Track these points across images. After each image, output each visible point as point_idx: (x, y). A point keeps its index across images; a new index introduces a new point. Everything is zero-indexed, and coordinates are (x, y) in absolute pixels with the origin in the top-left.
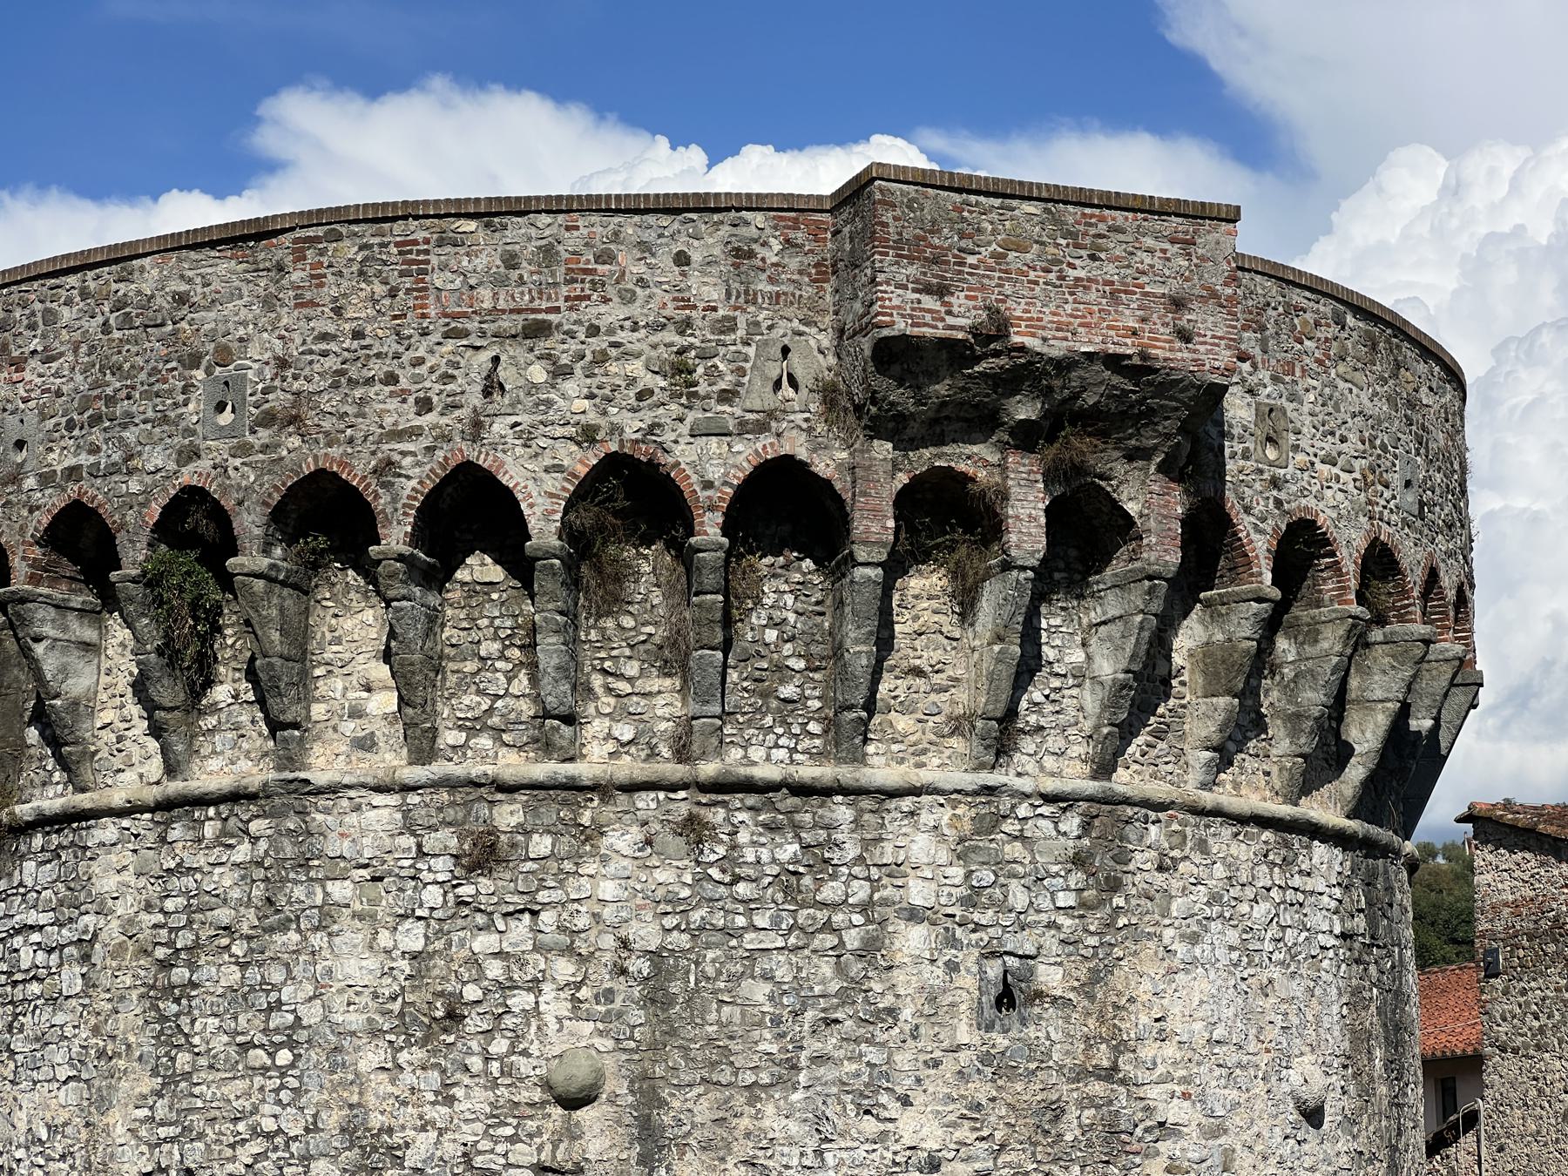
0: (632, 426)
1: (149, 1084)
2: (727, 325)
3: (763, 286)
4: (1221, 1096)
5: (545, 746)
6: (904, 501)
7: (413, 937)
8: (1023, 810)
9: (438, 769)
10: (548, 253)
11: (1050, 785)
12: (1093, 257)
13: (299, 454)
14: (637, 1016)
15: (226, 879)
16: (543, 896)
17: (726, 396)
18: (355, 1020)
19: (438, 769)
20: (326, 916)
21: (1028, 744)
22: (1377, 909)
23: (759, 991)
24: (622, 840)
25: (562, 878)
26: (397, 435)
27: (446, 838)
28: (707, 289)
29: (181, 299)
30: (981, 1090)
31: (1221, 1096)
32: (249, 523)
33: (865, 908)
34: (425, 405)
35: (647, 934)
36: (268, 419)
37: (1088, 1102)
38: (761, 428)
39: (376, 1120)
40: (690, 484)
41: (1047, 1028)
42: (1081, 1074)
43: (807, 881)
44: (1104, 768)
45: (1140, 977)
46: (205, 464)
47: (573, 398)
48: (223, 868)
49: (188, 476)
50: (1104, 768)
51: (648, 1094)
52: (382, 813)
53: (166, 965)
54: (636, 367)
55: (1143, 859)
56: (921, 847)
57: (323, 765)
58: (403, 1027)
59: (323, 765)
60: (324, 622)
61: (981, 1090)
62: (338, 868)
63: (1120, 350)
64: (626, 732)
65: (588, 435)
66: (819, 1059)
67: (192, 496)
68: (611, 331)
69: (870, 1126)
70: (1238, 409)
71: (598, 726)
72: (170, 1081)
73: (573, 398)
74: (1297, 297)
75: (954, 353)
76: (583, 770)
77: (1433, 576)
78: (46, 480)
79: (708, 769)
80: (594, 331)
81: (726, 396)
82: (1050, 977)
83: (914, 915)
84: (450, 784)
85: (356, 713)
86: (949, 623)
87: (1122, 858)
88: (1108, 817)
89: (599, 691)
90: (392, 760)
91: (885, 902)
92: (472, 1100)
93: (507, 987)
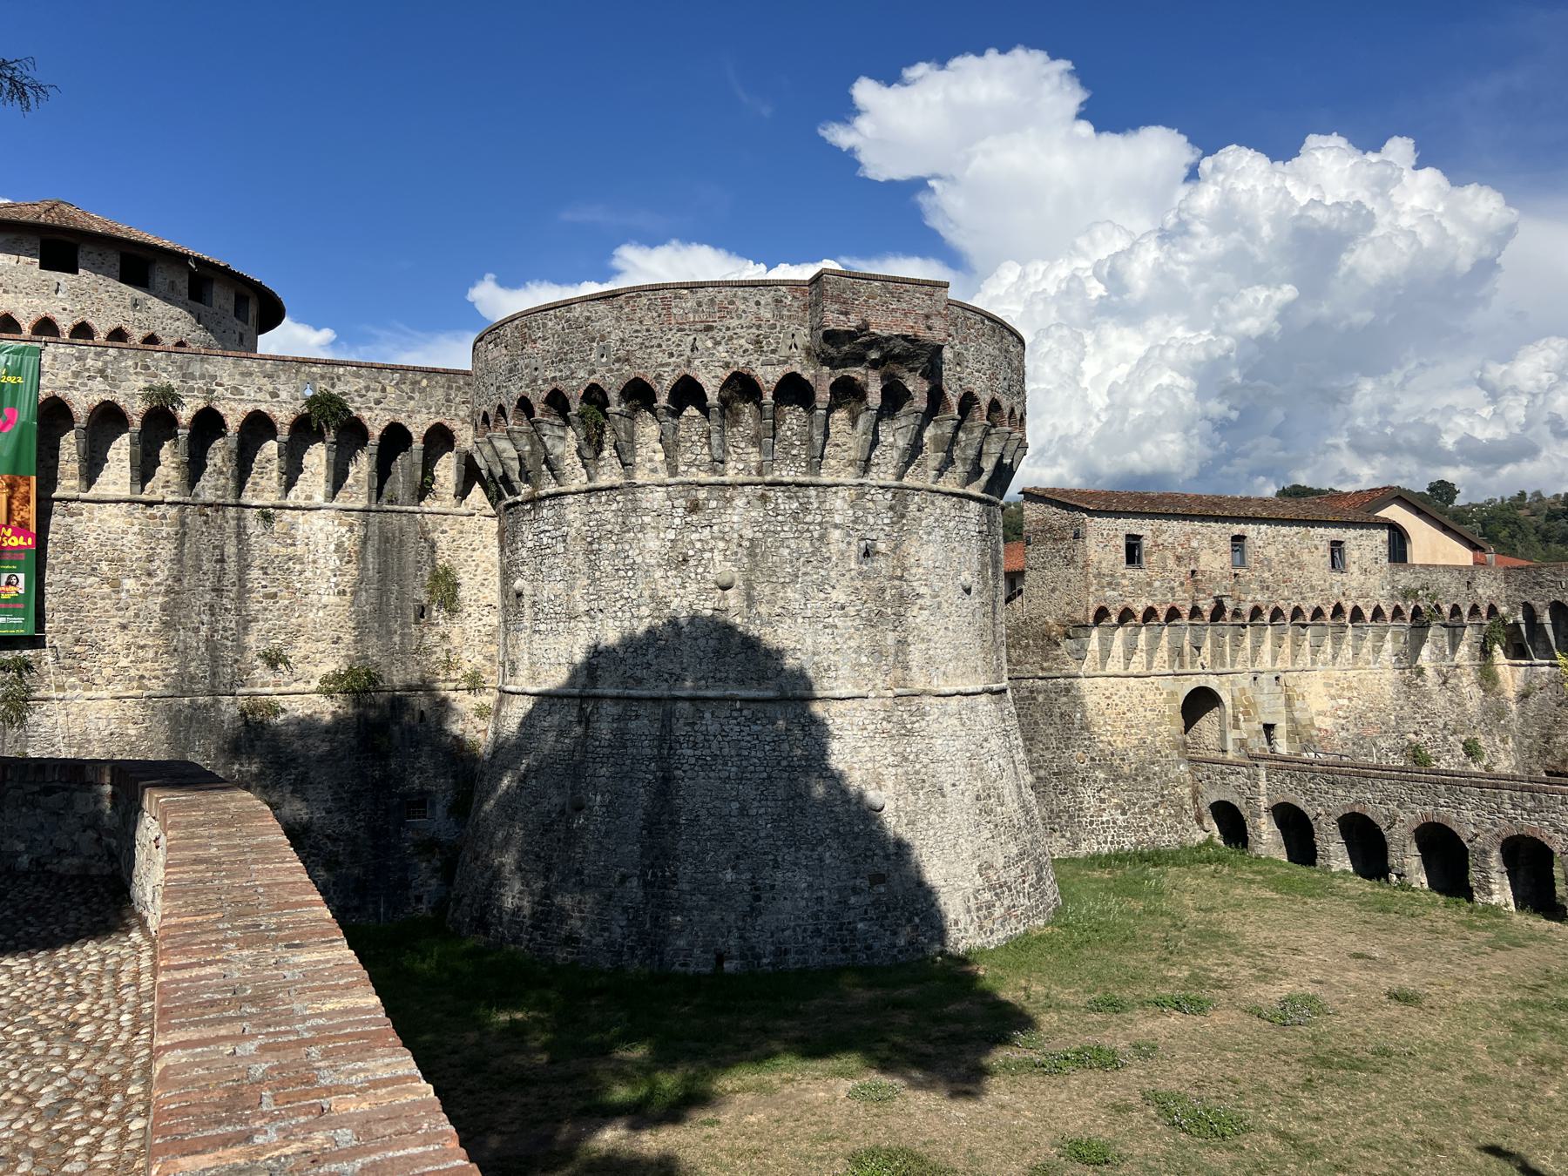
0: (742, 362)
1: (587, 582)
2: (773, 327)
3: (785, 313)
4: (937, 585)
5: (714, 471)
6: (833, 387)
7: (671, 535)
9: (678, 479)
10: (712, 301)
11: (882, 483)
13: (630, 372)
14: (745, 560)
15: (609, 515)
17: (773, 352)
18: (653, 562)
19: (678, 479)
20: (643, 527)
21: (874, 469)
22: (991, 523)
23: (786, 552)
24: (740, 502)
25: (720, 515)
26: (662, 365)
27: (682, 502)
28: (766, 314)
29: (588, 318)
30: (858, 584)
31: (937, 585)
32: (613, 396)
33: (820, 524)
34: (671, 355)
35: (748, 533)
36: (618, 360)
37: (894, 587)
38: (785, 362)
39: (661, 594)
40: (762, 382)
41: (880, 563)
42: (892, 578)
44: (900, 477)
45: (911, 547)
46: (597, 376)
47: (722, 352)
48: (608, 512)
49: (592, 380)
50: (900, 477)
51: (749, 585)
52: (660, 493)
53: (591, 543)
54: (742, 341)
55: (913, 507)
56: (839, 503)
57: (640, 477)
58: (668, 564)
59: (640, 477)
60: (639, 430)
61: (858, 584)
62: (646, 511)
64: (741, 466)
65: (727, 365)
66: (805, 574)
67: (594, 387)
69: (822, 595)
70: (947, 354)
71: (732, 464)
72: (594, 581)
73: (722, 352)
74: (968, 314)
75: (850, 336)
76: (727, 479)
77: (1012, 410)
78: (545, 381)
79: (768, 478)
80: (728, 329)
81: (773, 352)
82: (881, 547)
83: (836, 526)
84: (683, 484)
85: (651, 460)
86: (848, 429)
87: (906, 507)
88: (901, 493)
90: (663, 476)
92: (692, 587)
93: (703, 551)
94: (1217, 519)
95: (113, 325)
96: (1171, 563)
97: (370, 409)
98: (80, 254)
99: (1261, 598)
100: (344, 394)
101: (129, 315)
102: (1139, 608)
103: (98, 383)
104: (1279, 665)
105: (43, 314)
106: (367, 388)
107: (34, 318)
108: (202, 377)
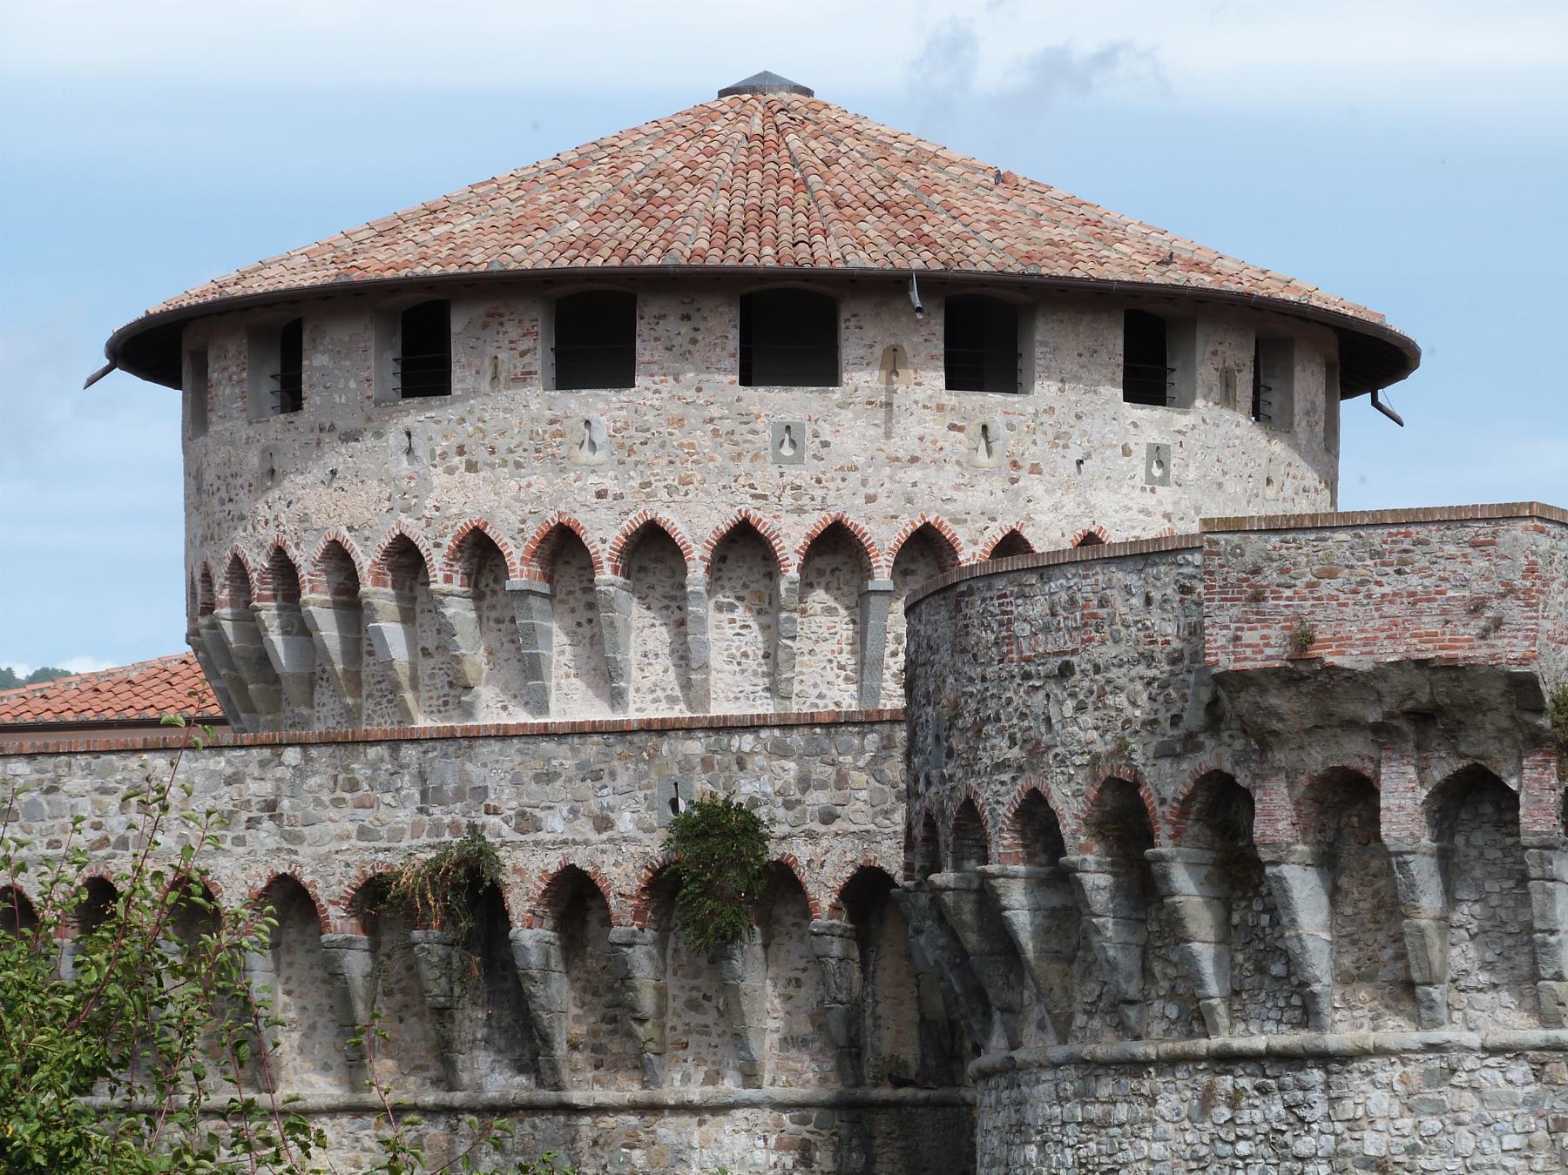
8: (1469, 1063)
9: (1073, 1047)
11: (1494, 1040)
12: (1399, 572)
16: (1120, 1157)
19: (1073, 1047)
43: (1288, 1137)
56: (1379, 1101)
63: (1422, 656)
68: (1107, 669)
89: (1158, 975)
91: (1345, 1153)
95: (719, 519)
97: (811, 836)
98: (640, 327)
100: (754, 802)
101: (766, 477)
103: (266, 835)
105: (552, 518)
106: (805, 783)
107: (533, 530)
108: (459, 795)
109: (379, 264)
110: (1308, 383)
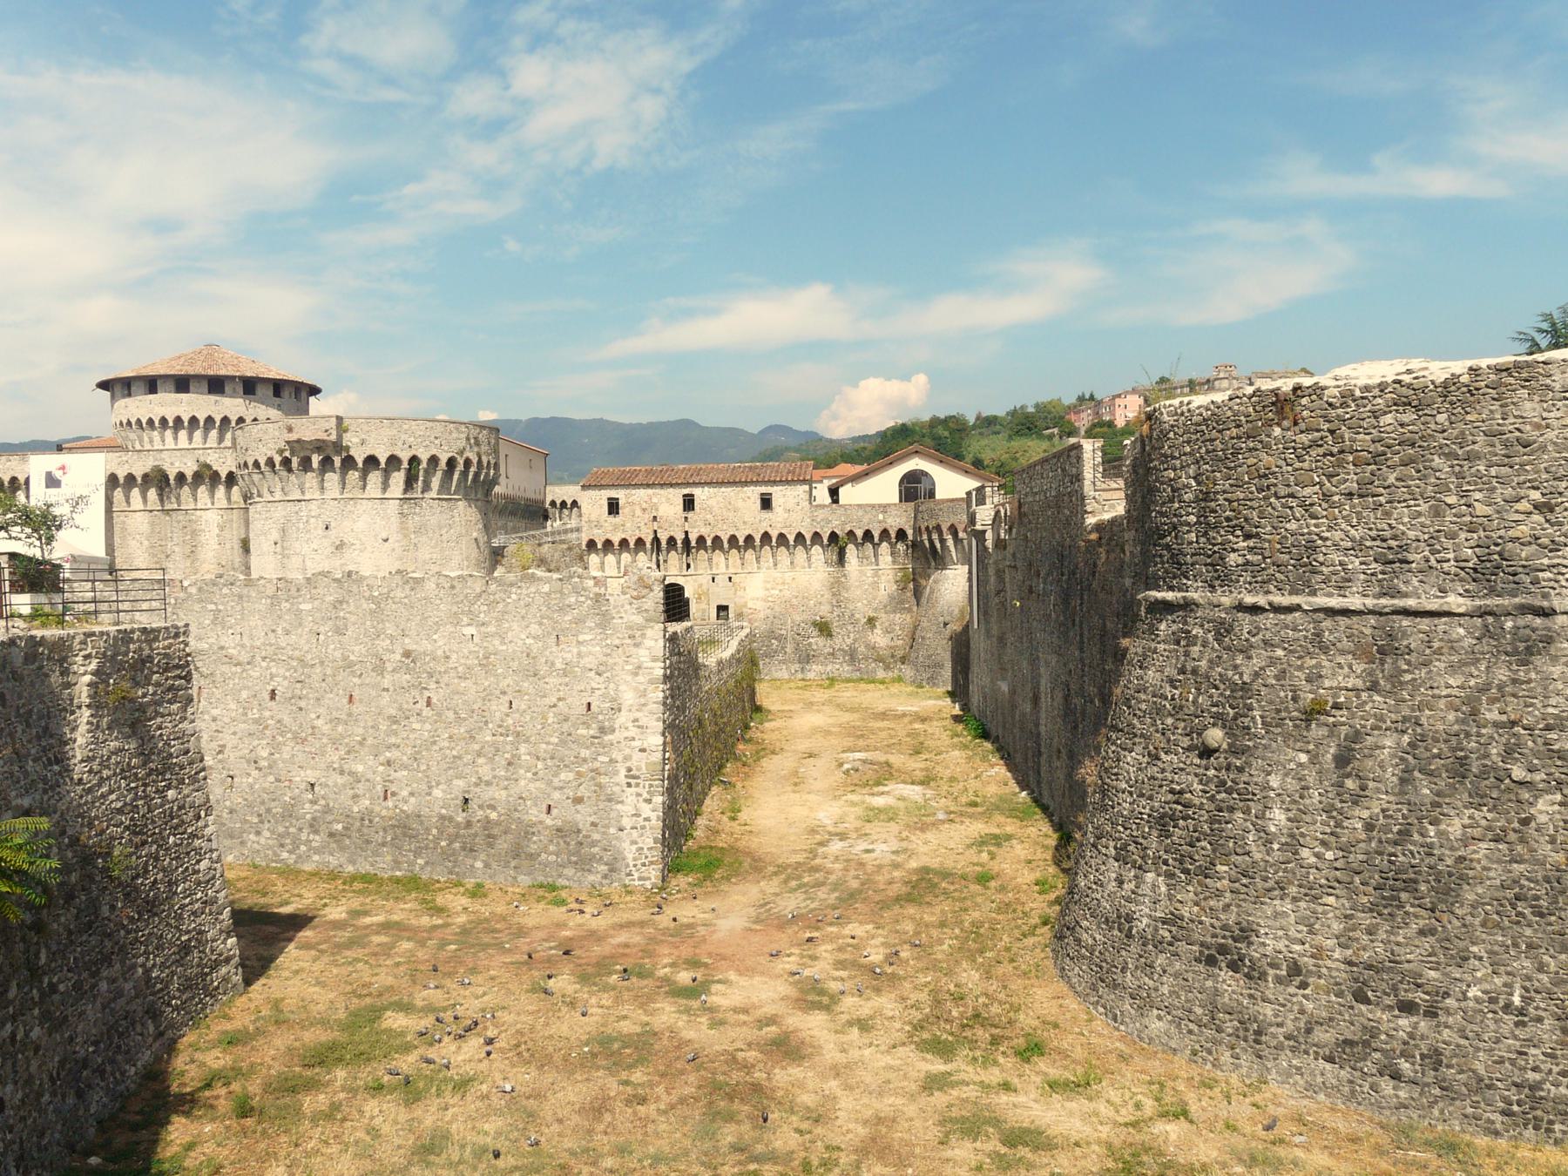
94: (671, 485)
96: (638, 512)
99: (704, 531)
102: (616, 540)
104: (732, 570)
109: (144, 372)
110: (304, 394)
